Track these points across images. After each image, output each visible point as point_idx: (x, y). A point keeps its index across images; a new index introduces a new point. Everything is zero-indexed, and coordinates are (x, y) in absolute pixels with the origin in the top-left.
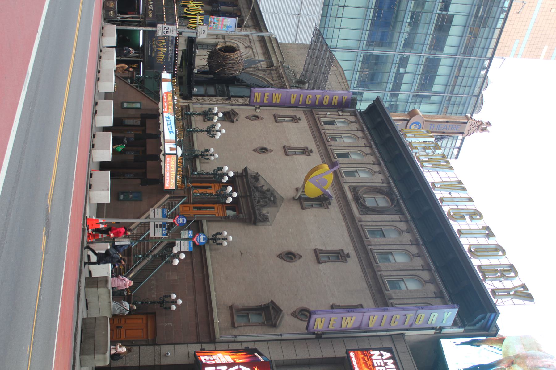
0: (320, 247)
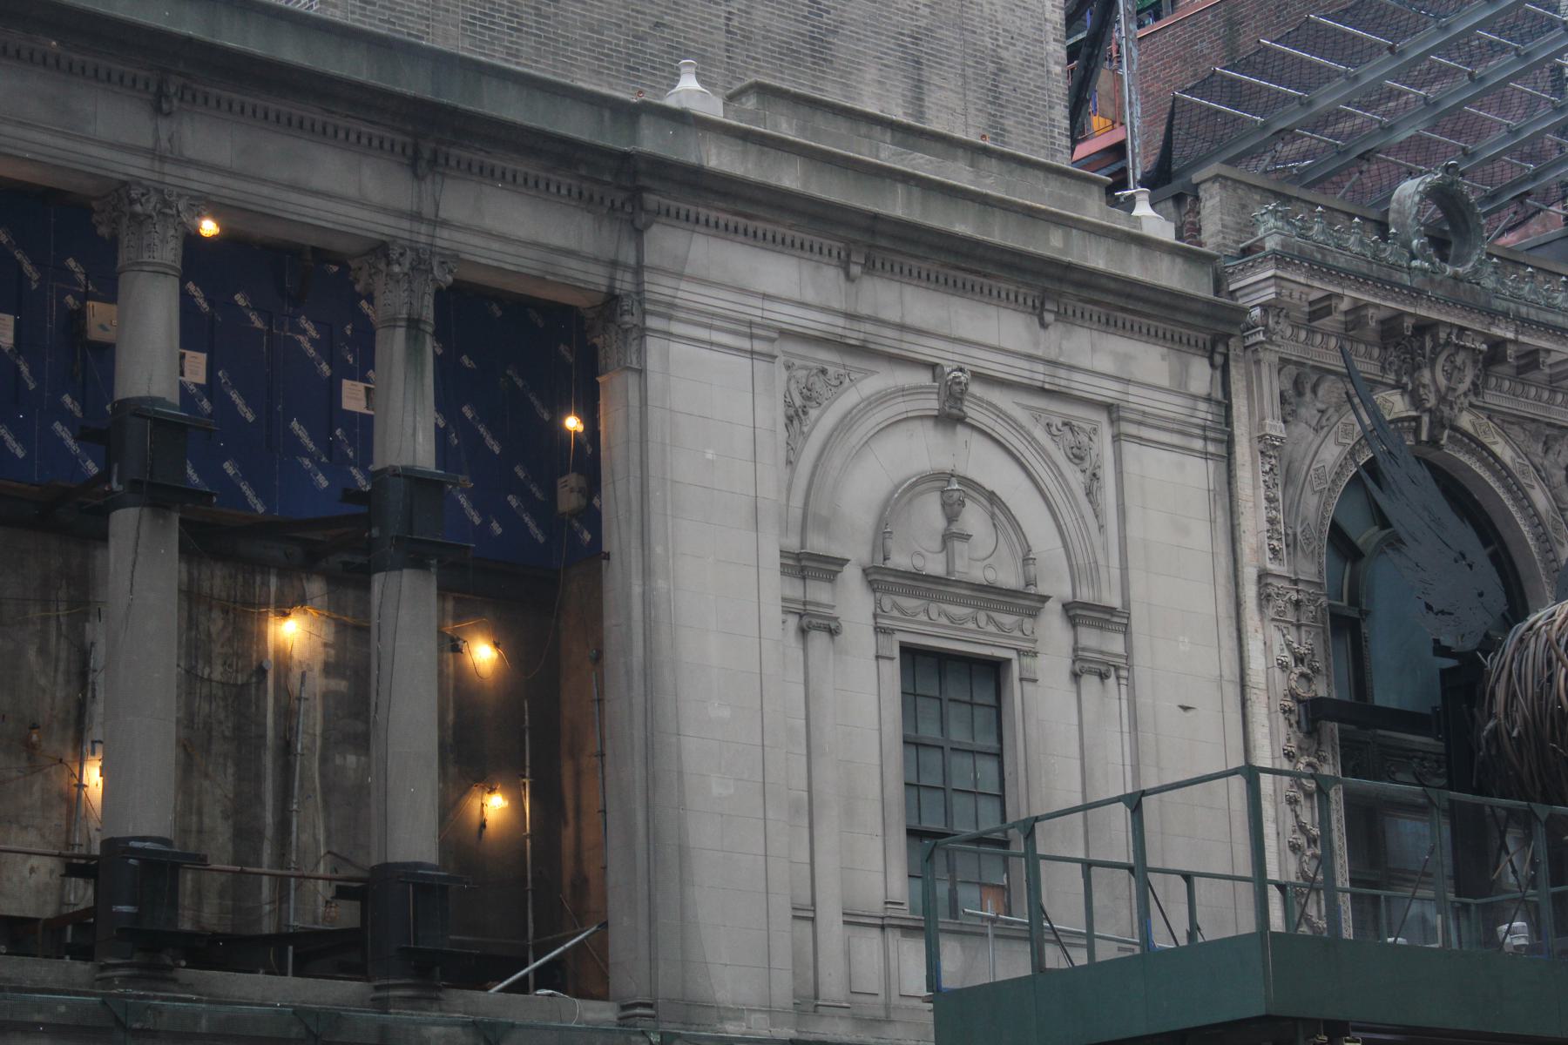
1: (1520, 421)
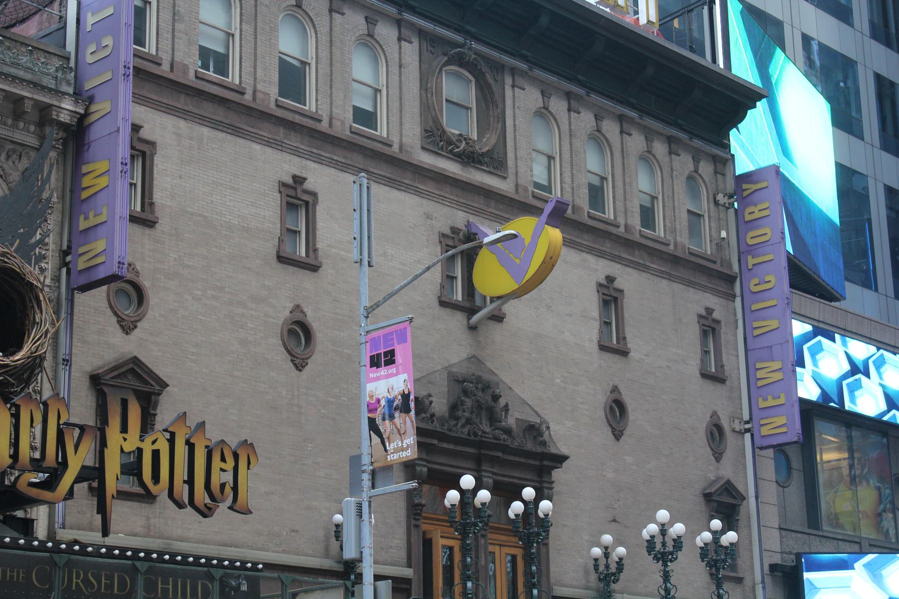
0: (594, 334)
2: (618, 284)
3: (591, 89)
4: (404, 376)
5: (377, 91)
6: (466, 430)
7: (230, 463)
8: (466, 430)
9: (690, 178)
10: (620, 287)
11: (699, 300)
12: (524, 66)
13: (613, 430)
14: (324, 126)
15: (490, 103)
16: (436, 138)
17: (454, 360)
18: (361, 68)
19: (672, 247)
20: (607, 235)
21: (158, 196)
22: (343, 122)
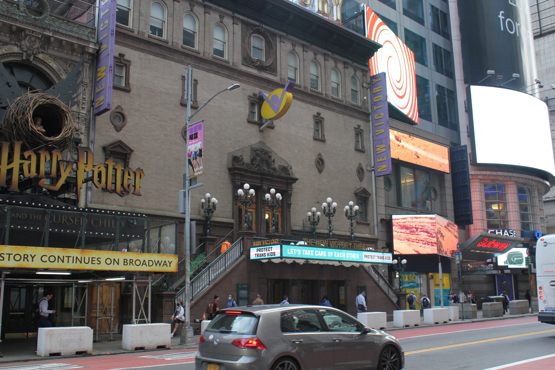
1: (61, 58)
2: (322, 116)
3: (312, 43)
4: (200, 143)
5: (225, 43)
6: (257, 169)
7: (132, 177)
8: (257, 169)
9: (353, 77)
10: (323, 117)
11: (354, 122)
12: (285, 34)
13: (319, 170)
14: (201, 55)
15: (270, 48)
16: (247, 60)
17: (254, 143)
18: (218, 34)
19: (344, 102)
20: (318, 98)
21: (131, 81)
22: (209, 54)
